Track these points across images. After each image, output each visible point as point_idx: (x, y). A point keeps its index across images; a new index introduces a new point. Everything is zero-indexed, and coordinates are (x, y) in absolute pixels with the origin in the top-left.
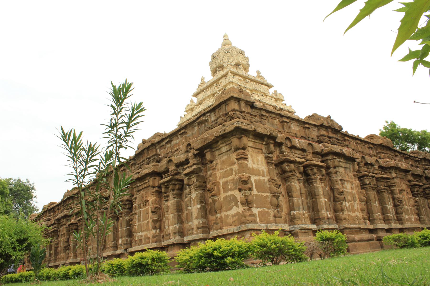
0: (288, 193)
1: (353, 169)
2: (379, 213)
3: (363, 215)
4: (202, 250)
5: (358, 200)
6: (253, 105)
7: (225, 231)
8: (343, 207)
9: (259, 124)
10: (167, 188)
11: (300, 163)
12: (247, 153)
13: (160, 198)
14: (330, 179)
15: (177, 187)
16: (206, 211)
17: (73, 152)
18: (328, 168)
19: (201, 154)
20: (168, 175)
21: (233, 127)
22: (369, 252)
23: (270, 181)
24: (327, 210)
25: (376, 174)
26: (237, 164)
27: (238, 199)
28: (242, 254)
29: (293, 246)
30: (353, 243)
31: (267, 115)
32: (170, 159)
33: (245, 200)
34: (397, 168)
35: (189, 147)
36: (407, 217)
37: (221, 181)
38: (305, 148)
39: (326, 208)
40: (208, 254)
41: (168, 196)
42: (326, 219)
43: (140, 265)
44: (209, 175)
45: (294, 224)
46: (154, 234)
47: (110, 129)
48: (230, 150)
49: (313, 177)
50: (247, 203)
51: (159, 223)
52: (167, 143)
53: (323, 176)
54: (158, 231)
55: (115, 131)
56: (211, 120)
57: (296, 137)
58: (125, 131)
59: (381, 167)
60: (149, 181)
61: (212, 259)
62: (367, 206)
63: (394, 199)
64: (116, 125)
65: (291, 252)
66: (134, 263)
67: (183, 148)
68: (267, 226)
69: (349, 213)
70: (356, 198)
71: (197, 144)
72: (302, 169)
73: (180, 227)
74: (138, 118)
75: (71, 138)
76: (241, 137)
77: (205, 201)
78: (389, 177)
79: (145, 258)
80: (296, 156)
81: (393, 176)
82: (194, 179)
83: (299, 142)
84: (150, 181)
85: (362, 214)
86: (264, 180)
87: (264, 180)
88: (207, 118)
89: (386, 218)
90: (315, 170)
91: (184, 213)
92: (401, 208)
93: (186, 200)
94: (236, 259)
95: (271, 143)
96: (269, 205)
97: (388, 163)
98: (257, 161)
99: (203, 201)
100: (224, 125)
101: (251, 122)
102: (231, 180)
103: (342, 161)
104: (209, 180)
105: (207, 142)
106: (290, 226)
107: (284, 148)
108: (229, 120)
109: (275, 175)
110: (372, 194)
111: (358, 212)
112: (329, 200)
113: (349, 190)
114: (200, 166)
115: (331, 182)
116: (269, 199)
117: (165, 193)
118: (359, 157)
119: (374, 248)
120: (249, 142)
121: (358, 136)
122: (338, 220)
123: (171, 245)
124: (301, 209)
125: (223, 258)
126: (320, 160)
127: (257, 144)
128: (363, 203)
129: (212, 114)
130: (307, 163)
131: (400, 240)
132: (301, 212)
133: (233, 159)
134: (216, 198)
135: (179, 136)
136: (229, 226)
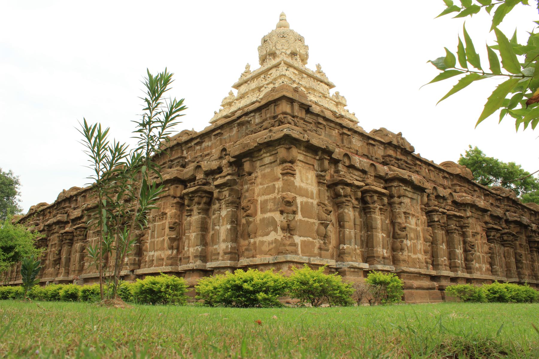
0: (339, 222)
1: (422, 201)
2: (445, 258)
3: (425, 259)
4: (229, 281)
5: (422, 239)
6: (308, 109)
7: (258, 260)
8: (404, 246)
9: (314, 134)
10: (191, 200)
11: (358, 187)
12: (295, 168)
13: (181, 212)
14: (392, 211)
15: (204, 200)
16: (237, 234)
17: (96, 151)
18: (391, 196)
19: (237, 162)
20: (194, 184)
21: (281, 135)
22: (428, 302)
23: (319, 205)
24: (383, 248)
25: (448, 210)
26: (281, 179)
27: (279, 223)
28: (277, 290)
29: (338, 287)
30: (410, 290)
31: (324, 123)
32: (199, 164)
33: (286, 226)
34: (473, 206)
35: (224, 153)
36: (477, 265)
37: (260, 199)
38: (367, 170)
39: (383, 245)
40: (236, 286)
41: (191, 210)
42: (381, 258)
43: (151, 291)
44: (245, 190)
45: (343, 260)
46: (169, 255)
47: (141, 128)
48: (274, 162)
49: (371, 206)
50: (289, 229)
51: (176, 243)
52: (196, 144)
53: (384, 205)
54: (175, 252)
55: (148, 130)
56: (254, 122)
57: (357, 154)
58: (159, 132)
59: (454, 202)
60: (169, 190)
61: (241, 292)
62: (432, 248)
63: (465, 242)
64: (149, 123)
65: (336, 294)
66: (143, 288)
67: (216, 152)
68: (309, 259)
69: (410, 254)
70: (420, 237)
71: (235, 150)
72: (359, 194)
73: (202, 249)
74: (177, 118)
75: (96, 134)
76: (290, 148)
77: (237, 221)
78: (463, 215)
79: (158, 283)
80: (353, 178)
81: (468, 215)
82: (226, 193)
83: (360, 161)
84: (172, 190)
85: (424, 257)
86: (312, 203)
87: (312, 203)
88: (249, 119)
89: (453, 265)
90: (375, 198)
91: (209, 232)
92: (472, 254)
93: (213, 217)
94: (270, 296)
95: (326, 159)
96: (315, 235)
97: (463, 198)
98: (306, 179)
99: (234, 221)
100: (270, 131)
101: (304, 130)
102: (272, 199)
103: (409, 189)
104: (245, 196)
105: (247, 149)
106: (337, 262)
107: (341, 167)
108: (278, 124)
109: (326, 198)
110: (440, 234)
111: (421, 253)
112: (388, 236)
113: (413, 226)
114: (235, 178)
115: (393, 215)
116: (316, 228)
117: (189, 206)
118: (430, 188)
119: (434, 299)
120: (299, 155)
121: (433, 161)
122: (395, 261)
123: (190, 270)
124: (353, 244)
125: (254, 292)
126: (382, 185)
127: (308, 158)
128: (428, 244)
129: (257, 114)
130: (367, 187)
131: (465, 292)
132: (353, 246)
133: (277, 173)
134: (251, 219)
135: (213, 137)
136: (263, 255)
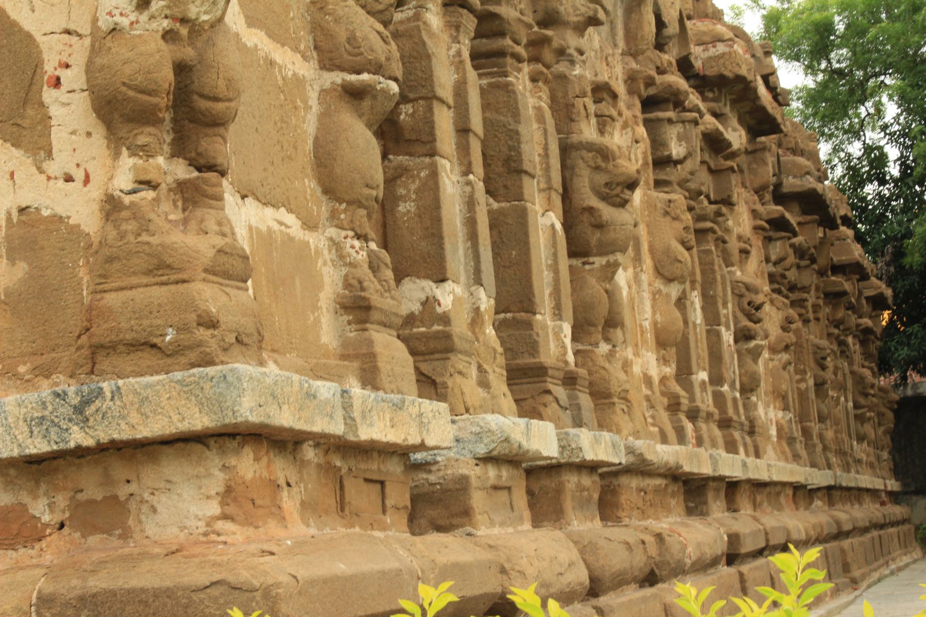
3: (663, 380)
33: (167, 76)
97: (721, 48)
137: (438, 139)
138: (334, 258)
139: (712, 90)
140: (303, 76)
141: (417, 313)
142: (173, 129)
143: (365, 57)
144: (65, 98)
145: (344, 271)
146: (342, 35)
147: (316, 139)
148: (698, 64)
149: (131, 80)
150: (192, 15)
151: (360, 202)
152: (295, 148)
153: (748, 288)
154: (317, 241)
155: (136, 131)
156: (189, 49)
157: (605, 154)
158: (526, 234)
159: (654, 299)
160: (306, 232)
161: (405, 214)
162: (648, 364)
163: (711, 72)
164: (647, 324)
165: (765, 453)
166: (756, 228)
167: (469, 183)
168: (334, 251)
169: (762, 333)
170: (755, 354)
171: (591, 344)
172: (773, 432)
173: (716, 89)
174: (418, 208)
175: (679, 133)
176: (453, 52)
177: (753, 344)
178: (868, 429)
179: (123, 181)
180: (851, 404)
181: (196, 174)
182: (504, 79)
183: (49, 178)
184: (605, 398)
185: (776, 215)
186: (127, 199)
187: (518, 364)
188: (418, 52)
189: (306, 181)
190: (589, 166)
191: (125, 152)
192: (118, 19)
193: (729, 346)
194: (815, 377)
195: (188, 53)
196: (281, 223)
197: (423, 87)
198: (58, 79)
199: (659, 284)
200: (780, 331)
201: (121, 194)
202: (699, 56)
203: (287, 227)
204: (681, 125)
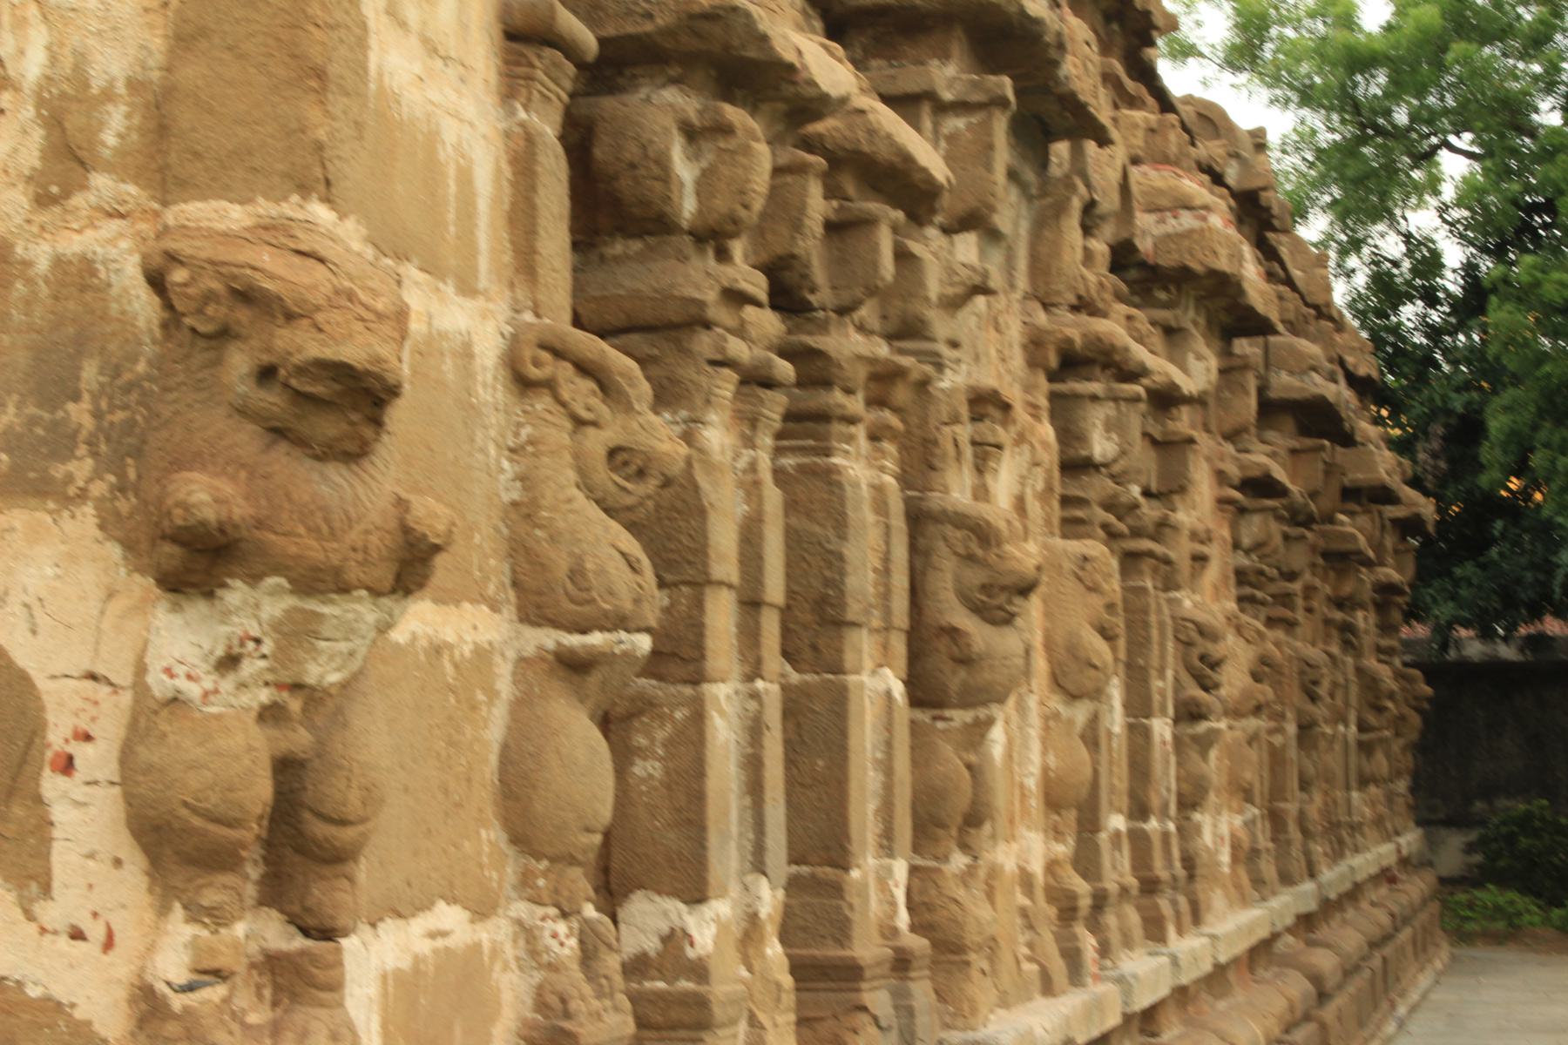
3: (1051, 866)
33: (262, 790)
97: (1187, 220)
137: (709, 654)
138: (522, 954)
139: (1167, 290)
140: (490, 644)
141: (652, 954)
142: (265, 859)
143: (599, 607)
144: (80, 792)
145: (538, 977)
146: (561, 563)
147: (505, 748)
148: (1145, 245)
149: (198, 800)
150: (311, 680)
151: (573, 857)
152: (469, 780)
153: (1202, 630)
154: (496, 933)
155: (200, 881)
156: (302, 731)
157: (983, 534)
158: (844, 733)
159: (1046, 728)
160: (478, 926)
161: (643, 780)
162: (1026, 848)
163: (1167, 261)
164: (1032, 783)
165: (1209, 908)
166: (1222, 502)
167: (755, 696)
168: (522, 943)
169: (1218, 707)
170: (1204, 743)
171: (937, 858)
172: (1225, 857)
173: (1172, 288)
174: (667, 773)
175: (1108, 417)
176: (742, 463)
177: (1202, 727)
178: (1380, 763)
179: (171, 965)
180: (1353, 728)
181: (299, 942)
182: (825, 459)
183: (43, 930)
184: (953, 952)
185: (1255, 473)
186: (177, 1002)
187: (814, 957)
188: (684, 501)
189: (483, 833)
190: (956, 554)
191: (178, 911)
192: (182, 683)
193: (1164, 743)
194: (1300, 713)
195: (300, 739)
196: (433, 935)
197: (689, 563)
198: (70, 758)
199: (1056, 703)
200: (1249, 680)
201: (167, 990)
202: (1148, 231)
203: (444, 934)
204: (1111, 404)
